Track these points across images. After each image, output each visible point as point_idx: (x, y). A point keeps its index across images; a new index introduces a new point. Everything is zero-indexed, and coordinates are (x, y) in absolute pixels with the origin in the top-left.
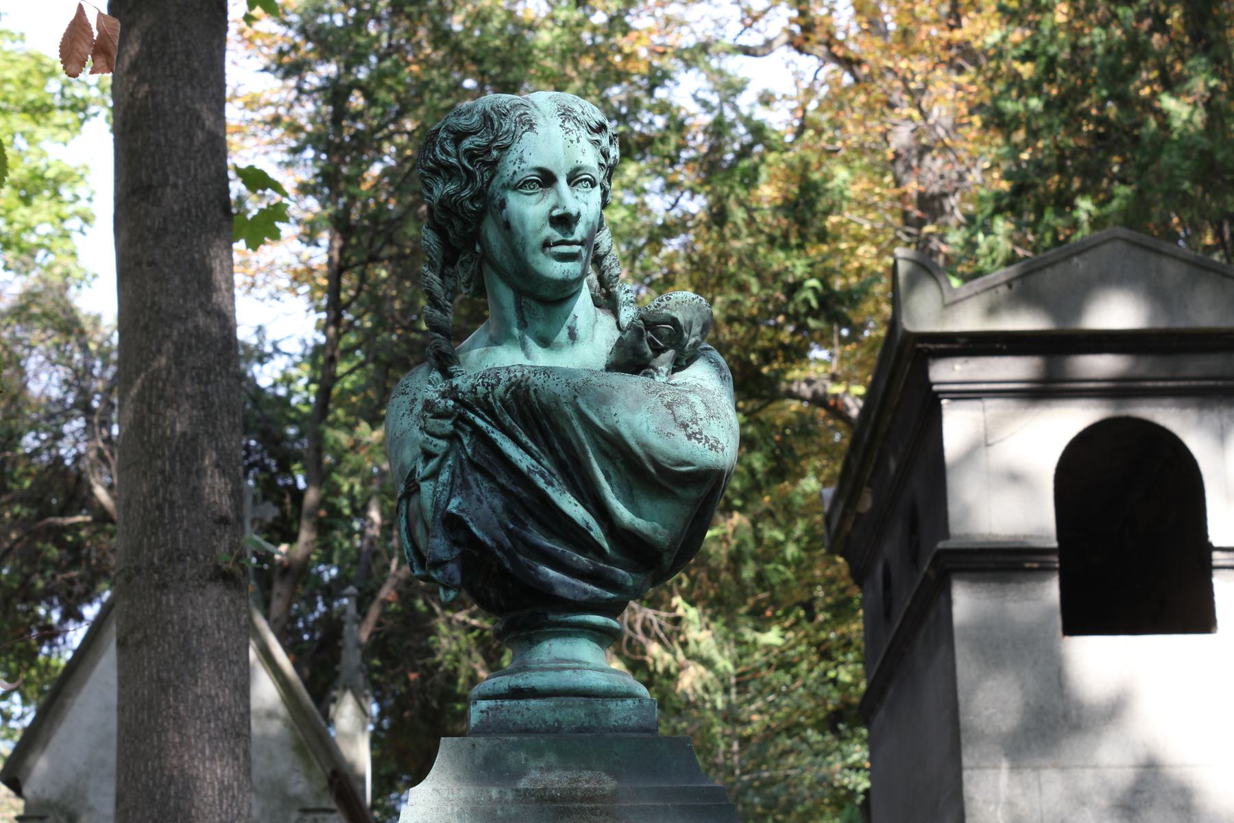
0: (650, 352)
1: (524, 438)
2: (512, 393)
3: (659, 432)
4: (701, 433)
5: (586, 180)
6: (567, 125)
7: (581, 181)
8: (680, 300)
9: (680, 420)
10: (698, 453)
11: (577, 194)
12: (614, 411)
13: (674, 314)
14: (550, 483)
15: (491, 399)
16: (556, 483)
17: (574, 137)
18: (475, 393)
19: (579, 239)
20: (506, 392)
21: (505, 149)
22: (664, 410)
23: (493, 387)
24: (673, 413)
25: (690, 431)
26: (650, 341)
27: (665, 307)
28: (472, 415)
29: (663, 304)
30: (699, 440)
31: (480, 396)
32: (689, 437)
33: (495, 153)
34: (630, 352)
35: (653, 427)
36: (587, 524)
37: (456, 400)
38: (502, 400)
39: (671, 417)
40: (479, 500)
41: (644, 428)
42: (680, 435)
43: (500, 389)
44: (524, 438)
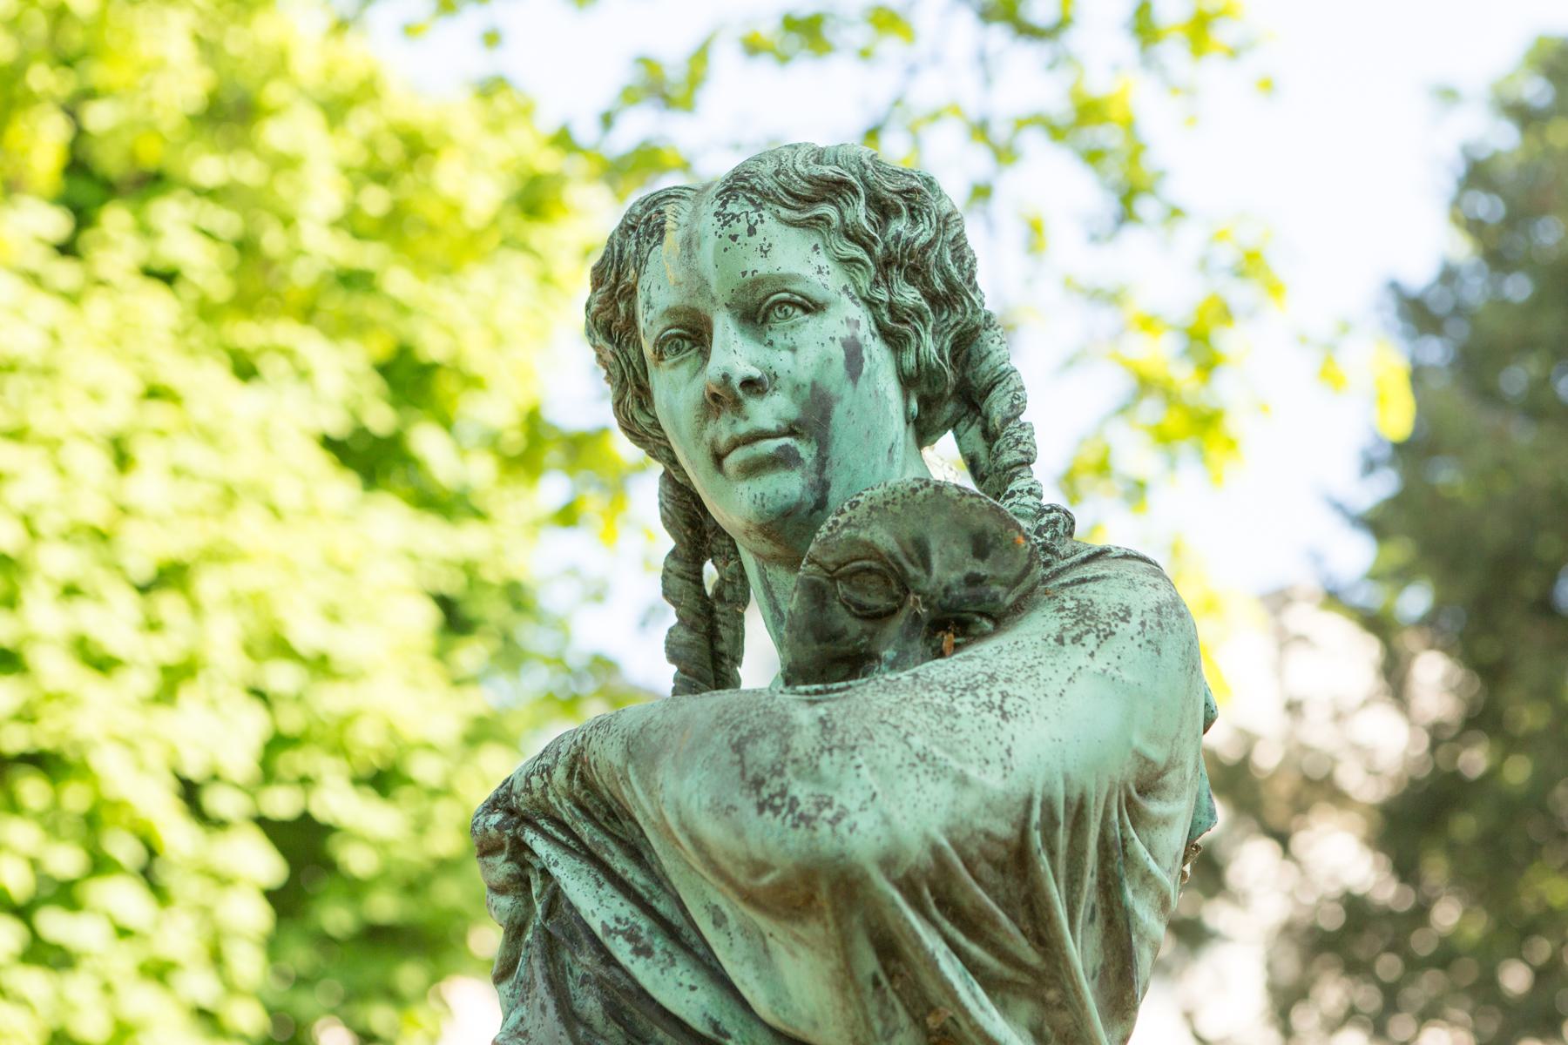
0: (854, 627)
1: (619, 863)
2: (582, 778)
3: (724, 811)
4: (783, 794)
5: (782, 302)
6: (732, 208)
7: (771, 307)
8: (879, 502)
9: (750, 775)
10: (772, 841)
11: (771, 336)
12: (660, 777)
13: (864, 535)
14: (644, 951)
15: (552, 799)
16: (657, 950)
17: (741, 228)
18: (529, 791)
19: (770, 424)
20: (570, 776)
21: (630, 293)
22: (727, 756)
23: (548, 770)
24: (742, 762)
25: (765, 793)
26: (847, 604)
27: (846, 525)
28: (529, 836)
29: (842, 520)
30: (776, 810)
31: (537, 795)
32: (761, 808)
33: (622, 306)
34: (809, 636)
35: (706, 802)
36: (715, 1026)
37: (511, 812)
38: (570, 796)
39: (737, 769)
40: (543, 1008)
41: (694, 805)
42: (746, 805)
43: (560, 774)
44: (619, 863)
